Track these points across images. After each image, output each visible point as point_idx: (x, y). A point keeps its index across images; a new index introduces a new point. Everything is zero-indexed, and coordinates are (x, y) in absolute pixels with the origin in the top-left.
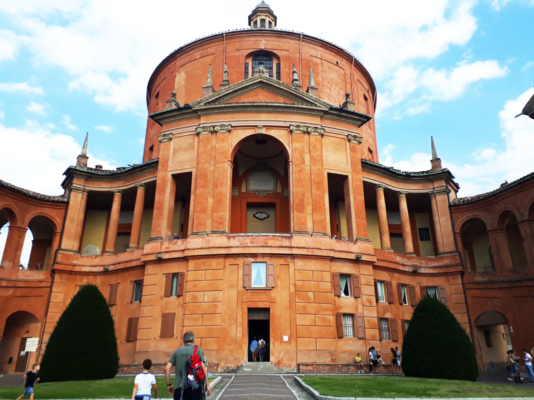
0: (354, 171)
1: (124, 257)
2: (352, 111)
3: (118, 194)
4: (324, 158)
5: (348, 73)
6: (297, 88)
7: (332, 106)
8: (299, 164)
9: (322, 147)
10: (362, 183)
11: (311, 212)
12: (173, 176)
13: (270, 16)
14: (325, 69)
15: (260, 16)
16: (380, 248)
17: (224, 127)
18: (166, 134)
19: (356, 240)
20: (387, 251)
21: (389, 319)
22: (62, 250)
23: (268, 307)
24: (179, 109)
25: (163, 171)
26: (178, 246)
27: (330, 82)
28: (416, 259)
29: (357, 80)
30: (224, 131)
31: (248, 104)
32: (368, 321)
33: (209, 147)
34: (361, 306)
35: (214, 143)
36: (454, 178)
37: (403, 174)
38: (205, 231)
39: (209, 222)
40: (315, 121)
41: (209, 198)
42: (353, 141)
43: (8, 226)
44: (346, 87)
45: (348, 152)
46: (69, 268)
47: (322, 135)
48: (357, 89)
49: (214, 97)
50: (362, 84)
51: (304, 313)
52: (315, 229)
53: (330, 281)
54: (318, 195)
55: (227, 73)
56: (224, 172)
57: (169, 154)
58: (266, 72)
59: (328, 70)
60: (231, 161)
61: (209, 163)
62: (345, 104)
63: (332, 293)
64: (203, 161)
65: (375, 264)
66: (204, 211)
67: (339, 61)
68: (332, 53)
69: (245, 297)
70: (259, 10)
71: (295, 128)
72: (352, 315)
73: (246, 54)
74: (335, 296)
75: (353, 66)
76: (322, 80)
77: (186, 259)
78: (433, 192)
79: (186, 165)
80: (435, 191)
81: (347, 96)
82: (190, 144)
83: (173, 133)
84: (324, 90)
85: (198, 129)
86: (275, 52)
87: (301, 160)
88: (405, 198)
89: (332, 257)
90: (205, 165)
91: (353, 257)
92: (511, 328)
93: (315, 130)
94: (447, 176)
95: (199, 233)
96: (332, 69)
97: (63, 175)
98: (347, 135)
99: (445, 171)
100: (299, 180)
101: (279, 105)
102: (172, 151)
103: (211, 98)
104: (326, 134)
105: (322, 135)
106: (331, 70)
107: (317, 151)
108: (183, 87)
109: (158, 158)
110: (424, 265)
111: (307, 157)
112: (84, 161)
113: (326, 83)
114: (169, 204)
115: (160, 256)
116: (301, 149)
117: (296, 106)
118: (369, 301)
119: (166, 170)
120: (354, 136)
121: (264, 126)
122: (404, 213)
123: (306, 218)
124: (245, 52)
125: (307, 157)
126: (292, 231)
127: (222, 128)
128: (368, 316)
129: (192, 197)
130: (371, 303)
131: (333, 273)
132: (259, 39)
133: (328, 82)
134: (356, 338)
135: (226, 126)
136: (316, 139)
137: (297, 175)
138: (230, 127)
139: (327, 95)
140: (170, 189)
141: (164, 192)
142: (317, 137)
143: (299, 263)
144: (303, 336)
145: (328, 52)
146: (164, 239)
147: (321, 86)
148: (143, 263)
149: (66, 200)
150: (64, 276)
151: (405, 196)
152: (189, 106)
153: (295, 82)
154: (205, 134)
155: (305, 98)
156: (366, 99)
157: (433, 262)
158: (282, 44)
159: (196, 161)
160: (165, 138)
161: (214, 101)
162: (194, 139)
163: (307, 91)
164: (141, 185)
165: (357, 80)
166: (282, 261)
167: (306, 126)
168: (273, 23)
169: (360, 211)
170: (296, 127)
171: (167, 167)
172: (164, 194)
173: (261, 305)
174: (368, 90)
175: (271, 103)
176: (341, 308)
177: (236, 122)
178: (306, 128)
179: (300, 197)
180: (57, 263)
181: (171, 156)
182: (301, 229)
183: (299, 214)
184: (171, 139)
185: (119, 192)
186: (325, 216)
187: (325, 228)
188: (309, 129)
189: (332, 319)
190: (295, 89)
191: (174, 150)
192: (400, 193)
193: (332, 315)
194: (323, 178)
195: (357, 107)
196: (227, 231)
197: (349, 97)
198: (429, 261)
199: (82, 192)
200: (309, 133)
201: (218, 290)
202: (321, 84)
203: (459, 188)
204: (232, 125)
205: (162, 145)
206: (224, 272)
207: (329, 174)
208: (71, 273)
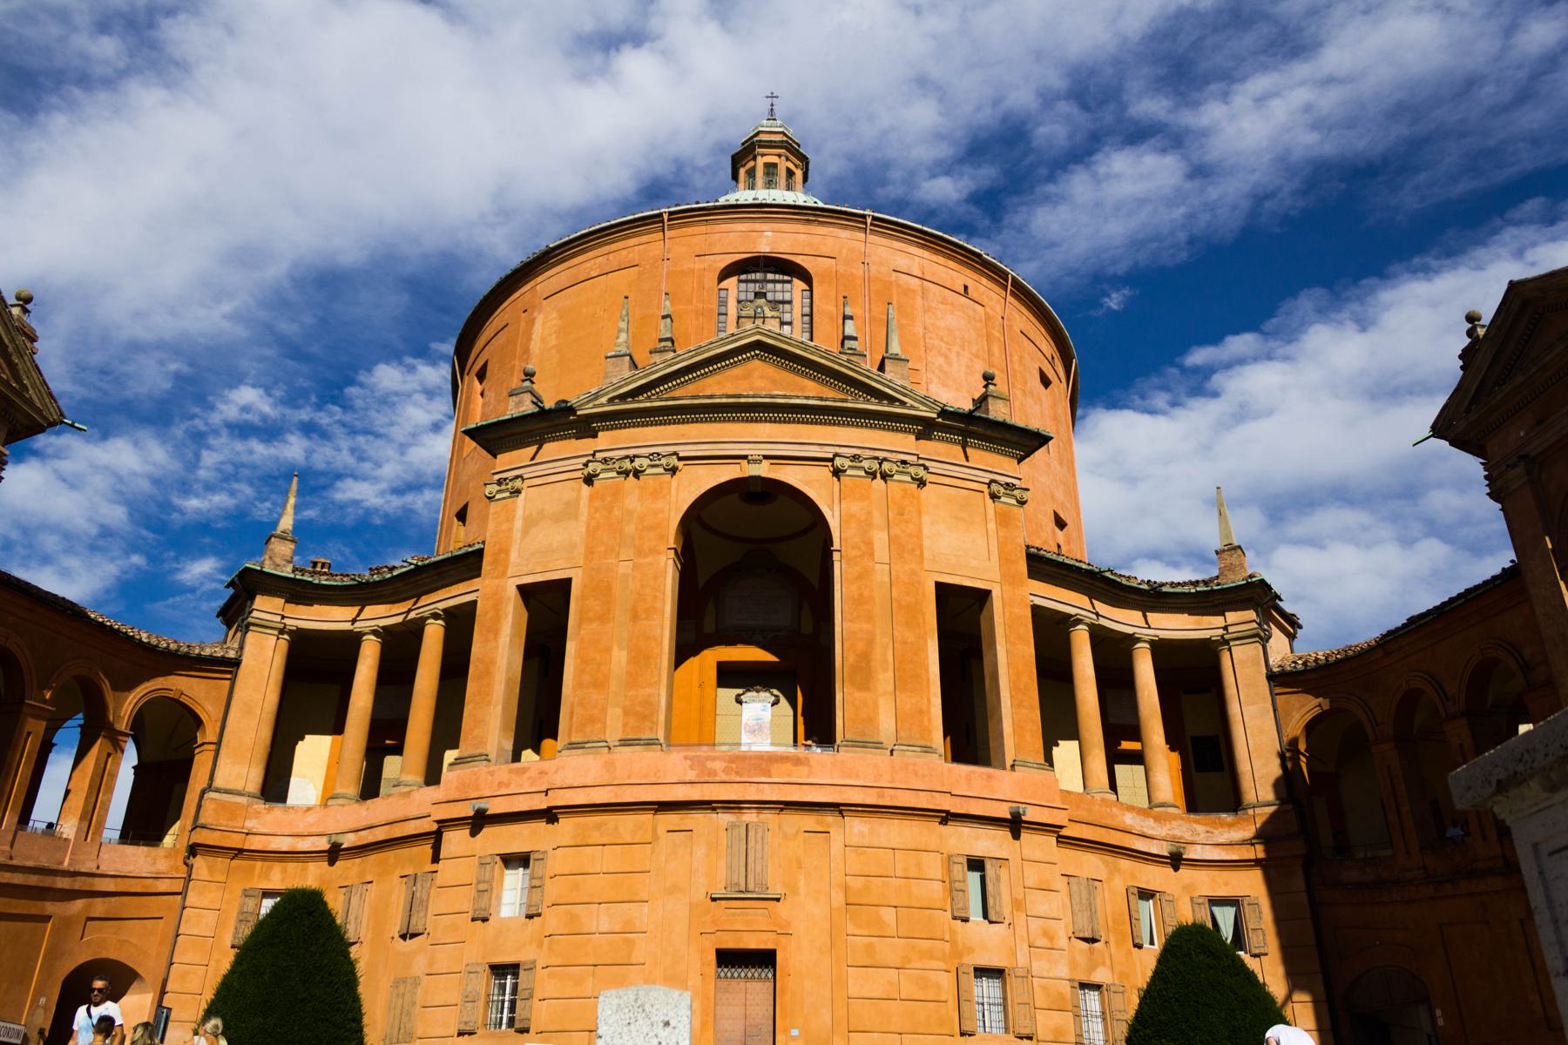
0: (1008, 578)
1: (377, 810)
2: (1000, 419)
3: (372, 637)
4: (926, 543)
5: (994, 314)
6: (852, 358)
7: (945, 405)
8: (860, 557)
9: (919, 513)
10: (1029, 610)
11: (891, 688)
12: (522, 589)
13: (791, 157)
14: (933, 305)
15: (763, 155)
16: (1080, 789)
17: (660, 460)
18: (505, 479)
19: (1013, 766)
20: (1098, 797)
21: (1105, 986)
22: (218, 790)
23: (770, 946)
24: (543, 414)
25: (495, 575)
26: (531, 778)
27: (945, 339)
28: (1180, 822)
29: (1021, 332)
30: (661, 470)
31: (724, 400)
32: (1044, 988)
33: (616, 513)
34: (1025, 946)
36: (1281, 600)
37: (1141, 587)
38: (603, 738)
40: (902, 443)
41: (615, 650)
42: (1003, 499)
43: (80, 726)
45: (992, 526)
46: (234, 841)
47: (922, 483)
48: (1021, 357)
49: (635, 381)
50: (1033, 342)
51: (868, 964)
52: (902, 734)
53: (940, 878)
54: (909, 640)
55: (669, 320)
56: (655, 578)
57: (510, 530)
58: (772, 317)
59: (941, 306)
60: (675, 549)
61: (618, 556)
62: (982, 401)
63: (945, 911)
64: (602, 549)
65: (1064, 832)
66: (600, 684)
67: (970, 284)
68: (951, 264)
69: (708, 918)
70: (760, 141)
71: (847, 463)
72: (997, 973)
73: (723, 265)
74: (955, 918)
75: (1010, 298)
76: (924, 334)
77: (550, 815)
78: (1222, 636)
79: (558, 560)
80: (1228, 633)
81: (988, 378)
82: (567, 504)
83: (525, 476)
84: (929, 359)
85: (590, 464)
86: (798, 260)
87: (863, 547)
88: (1149, 652)
89: (947, 812)
90: (606, 559)
91: (1004, 812)
92: (1438, 1013)
93: (901, 469)
94: (1258, 596)
95: (587, 745)
96: (952, 304)
97: (227, 587)
98: (987, 481)
99: (1254, 579)
100: (860, 601)
101: (805, 402)
102: (518, 524)
103: (627, 384)
104: (929, 478)
105: (922, 483)
106: (948, 307)
107: (907, 522)
108: (554, 351)
109: (484, 543)
110: (1200, 839)
111: (880, 538)
112: (283, 548)
113: (936, 342)
114: (509, 663)
115: (482, 804)
116: (863, 518)
117: (850, 405)
118: (1046, 934)
119: (504, 574)
120: (1007, 484)
121: (766, 457)
122: (1146, 693)
123: (876, 706)
124: (721, 261)
125: (880, 538)
126: (838, 742)
127: (653, 463)
128: (1045, 975)
129: (571, 647)
130: (1051, 939)
131: (949, 857)
132: (757, 226)
133: (942, 340)
134: (1011, 1037)
135: (664, 456)
136: (905, 490)
137: (854, 588)
138: (674, 461)
139: (937, 372)
140: (512, 626)
141: (496, 632)
142: (907, 485)
143: (857, 827)
144: (866, 1029)
145: (941, 260)
146: (493, 761)
147: (923, 349)
148: (435, 827)
149: (232, 654)
150: (221, 862)
151: (1148, 646)
152: (569, 404)
153: (848, 344)
154: (607, 477)
155: (873, 384)
156: (1046, 382)
157: (1226, 829)
158: (816, 240)
159: (581, 550)
160: (503, 487)
161: (634, 394)
162: (579, 490)
163: (881, 368)
164: (435, 616)
165: (1021, 332)
166: (809, 821)
167: (877, 458)
168: (799, 173)
169: (1022, 687)
170: (851, 461)
171: (506, 567)
172: (495, 639)
173: (752, 942)
174: (1053, 358)
175: (785, 397)
176: (971, 950)
177: (690, 447)
178: (876, 461)
179: (860, 646)
180: (203, 827)
181: (517, 535)
182: (864, 735)
183: (857, 694)
184: (518, 492)
185: (374, 632)
186: (929, 700)
187: (926, 731)
188: (886, 466)
189: (946, 981)
190: (848, 361)
191: (525, 520)
192: (1131, 640)
193: (946, 971)
194: (924, 594)
195: (1022, 404)
196: (662, 741)
197: (994, 382)
198: (1217, 829)
199: (276, 632)
200: (885, 477)
201: (637, 898)
202: (922, 344)
203: (1300, 627)
204: (681, 455)
205: (494, 506)
206: (653, 852)
207: (940, 586)
208: (239, 853)
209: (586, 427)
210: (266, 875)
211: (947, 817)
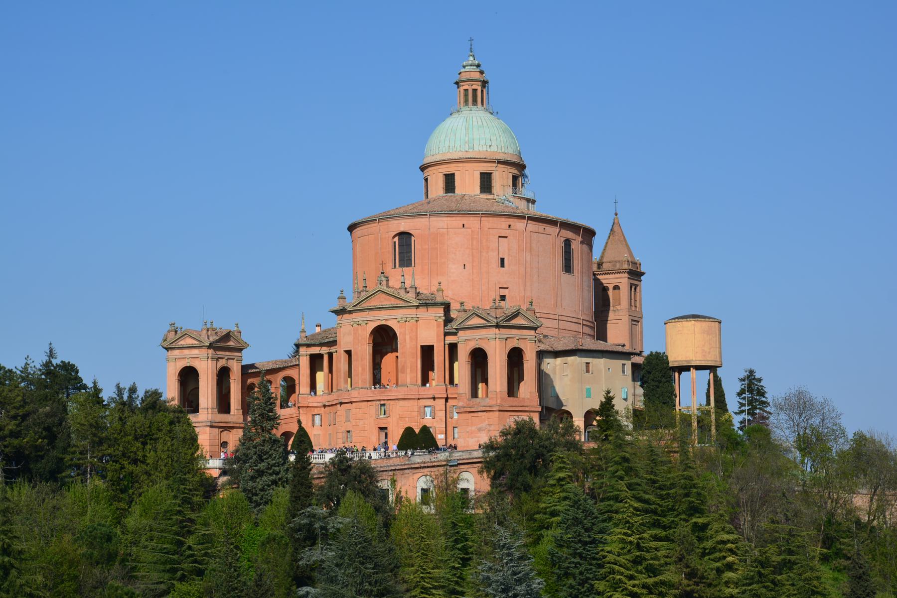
35: (360, 332)
39: (360, 382)
44: (472, 243)
45: (435, 328)
46: (306, 405)
77: (351, 403)
111: (408, 337)
125: (408, 337)
138: (366, 322)
143: (401, 403)
149: (297, 363)
150: (305, 409)
166: (393, 402)
209: (350, 312)
210: (314, 411)
211: (419, 399)
